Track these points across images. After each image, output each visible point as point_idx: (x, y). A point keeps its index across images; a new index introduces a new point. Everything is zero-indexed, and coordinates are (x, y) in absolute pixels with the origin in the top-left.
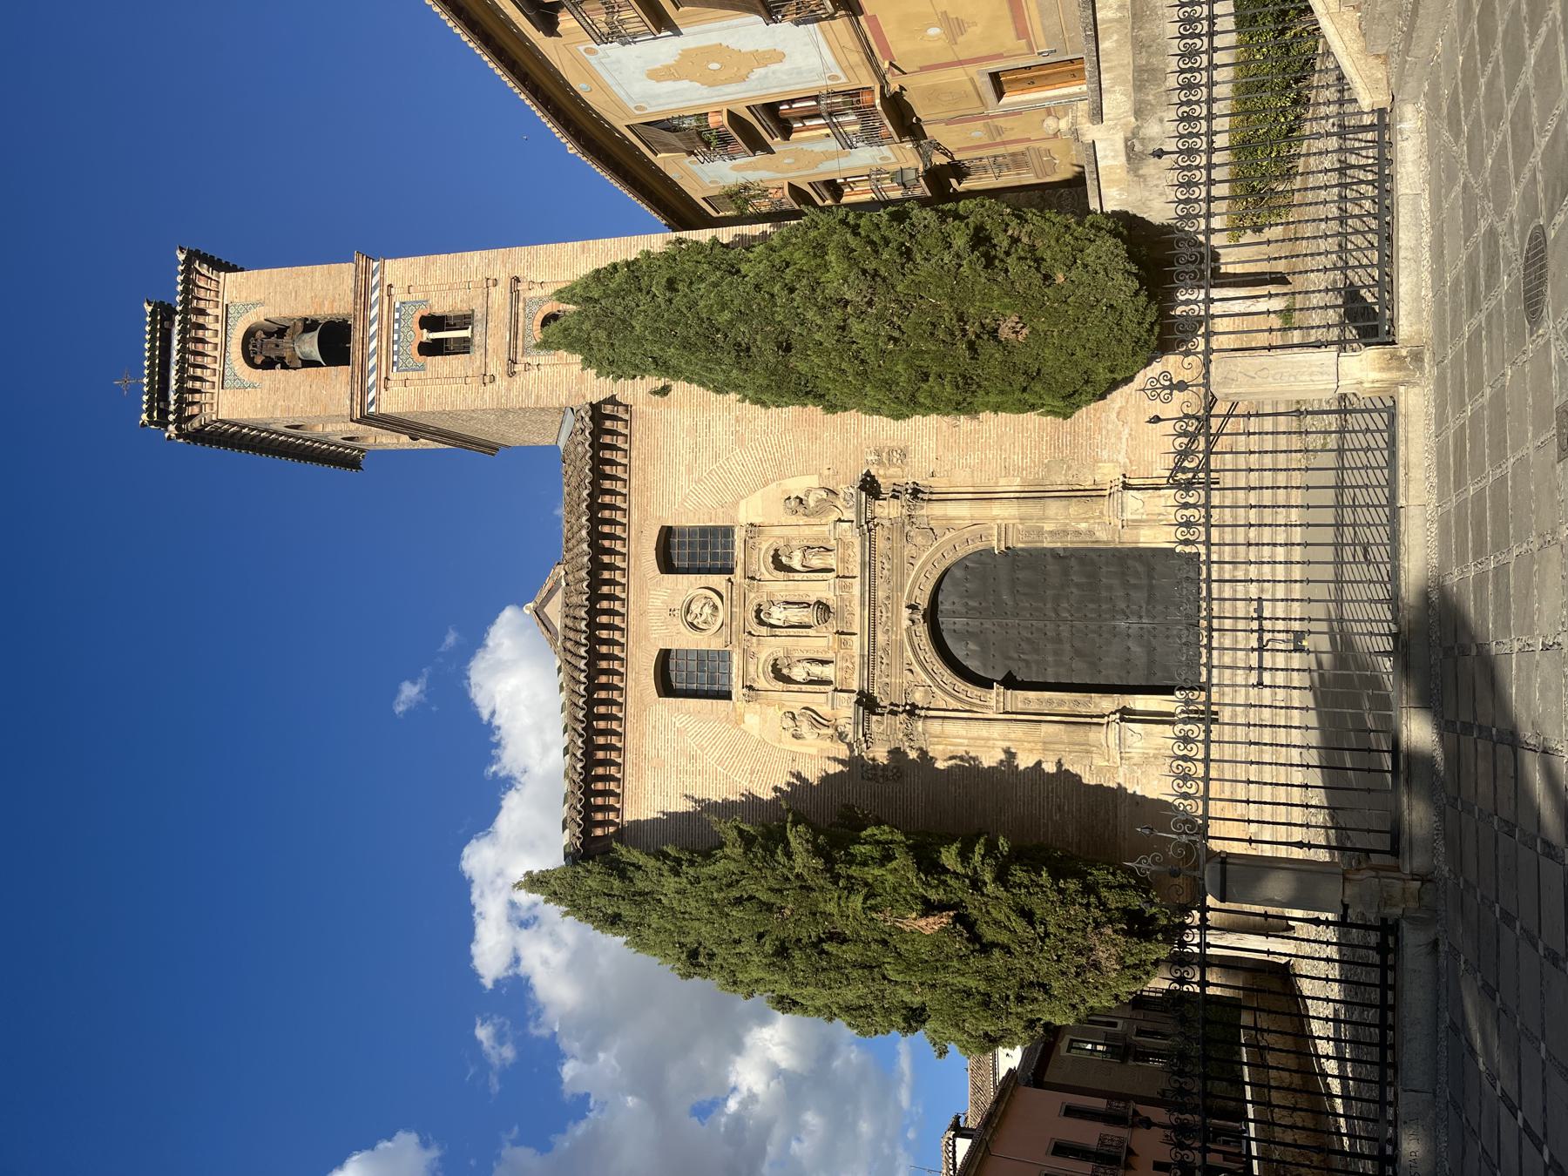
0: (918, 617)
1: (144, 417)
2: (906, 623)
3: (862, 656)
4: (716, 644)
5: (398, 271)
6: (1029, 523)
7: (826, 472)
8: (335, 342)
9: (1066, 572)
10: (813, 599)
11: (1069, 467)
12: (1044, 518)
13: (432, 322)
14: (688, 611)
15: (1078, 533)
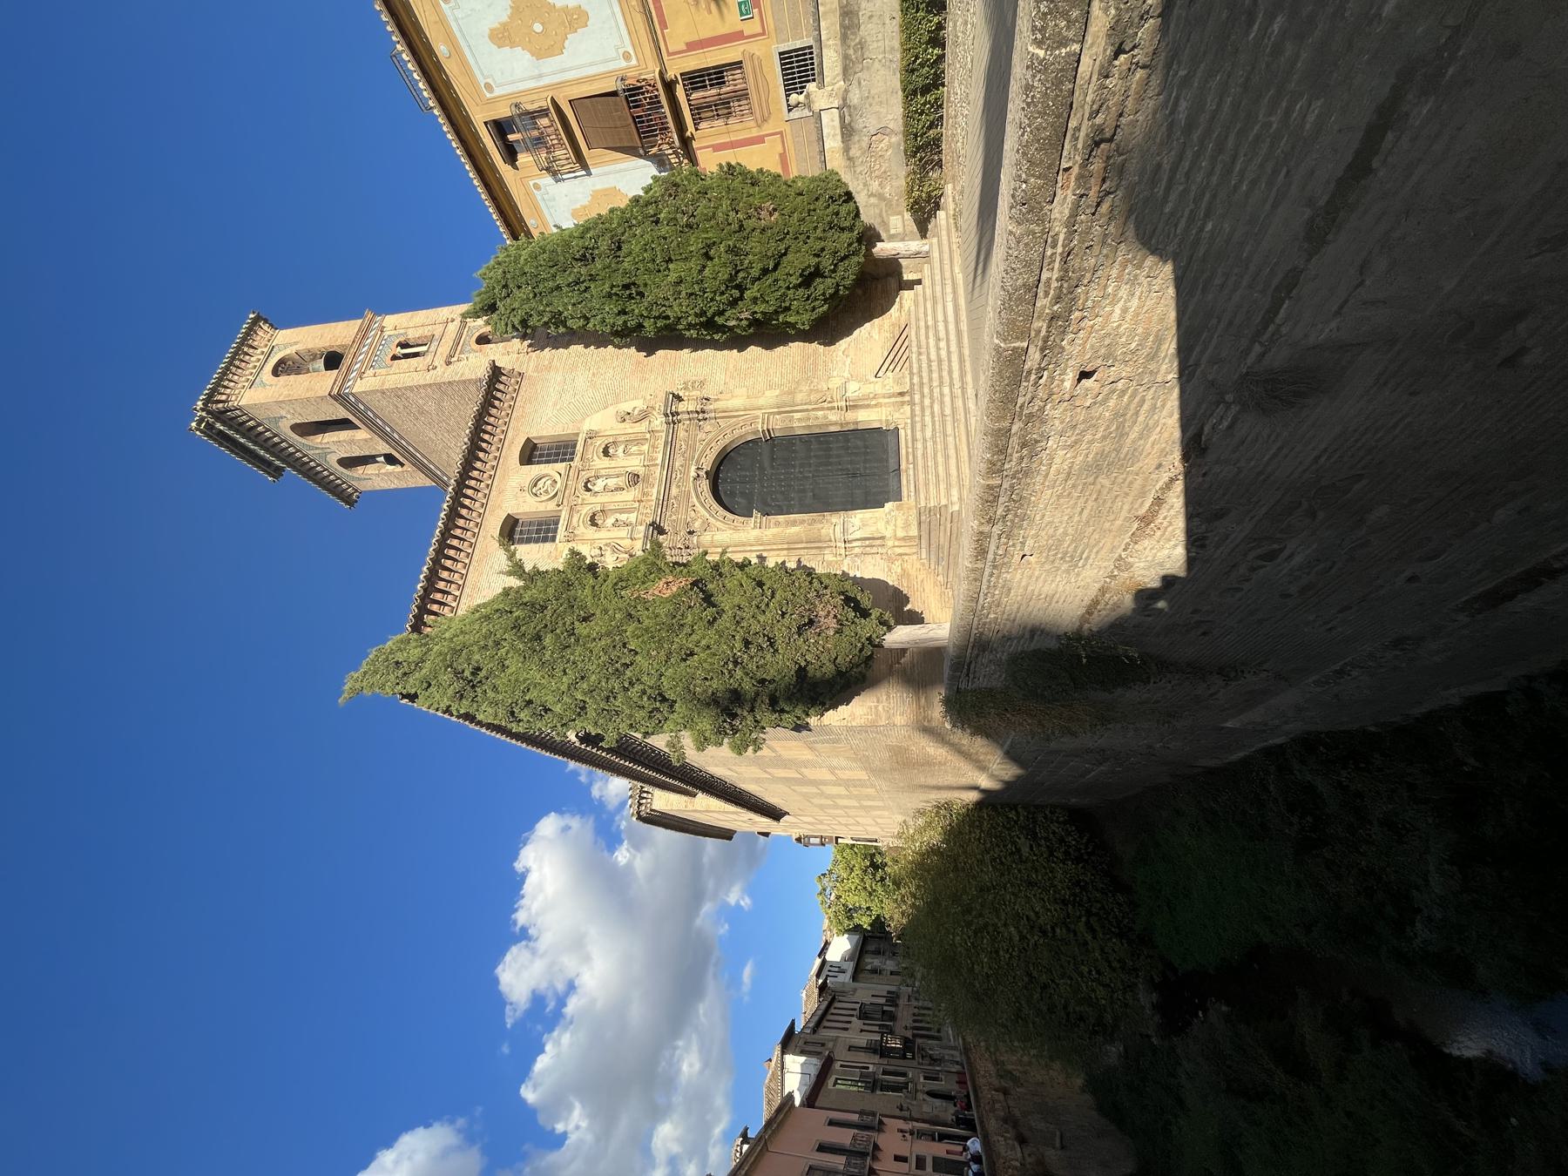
0: (702, 473)
1: (194, 424)
4: (551, 506)
5: (390, 321)
8: (333, 360)
13: (404, 345)
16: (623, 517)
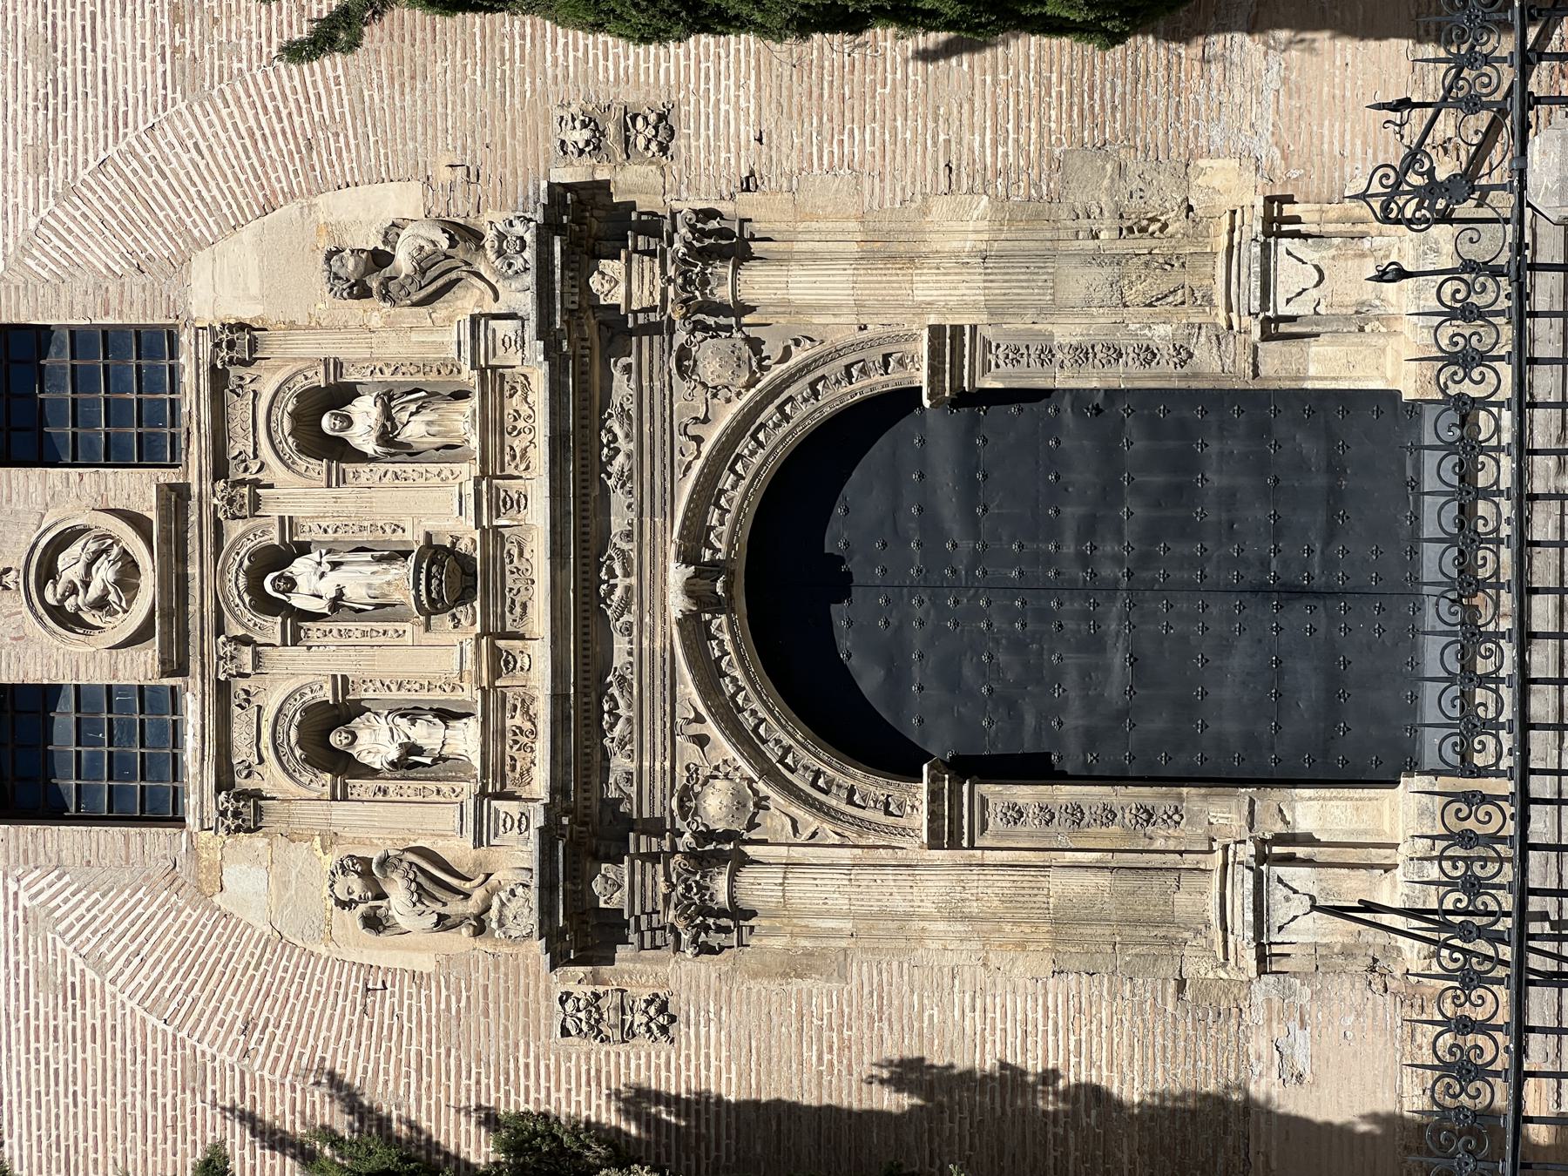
2: (677, 604)
3: (558, 698)
6: (1016, 324)
7: (445, 175)
9: (1109, 451)
10: (413, 537)
11: (1121, 169)
12: (1055, 308)
14: (48, 571)
15: (1149, 355)
16: (426, 734)
